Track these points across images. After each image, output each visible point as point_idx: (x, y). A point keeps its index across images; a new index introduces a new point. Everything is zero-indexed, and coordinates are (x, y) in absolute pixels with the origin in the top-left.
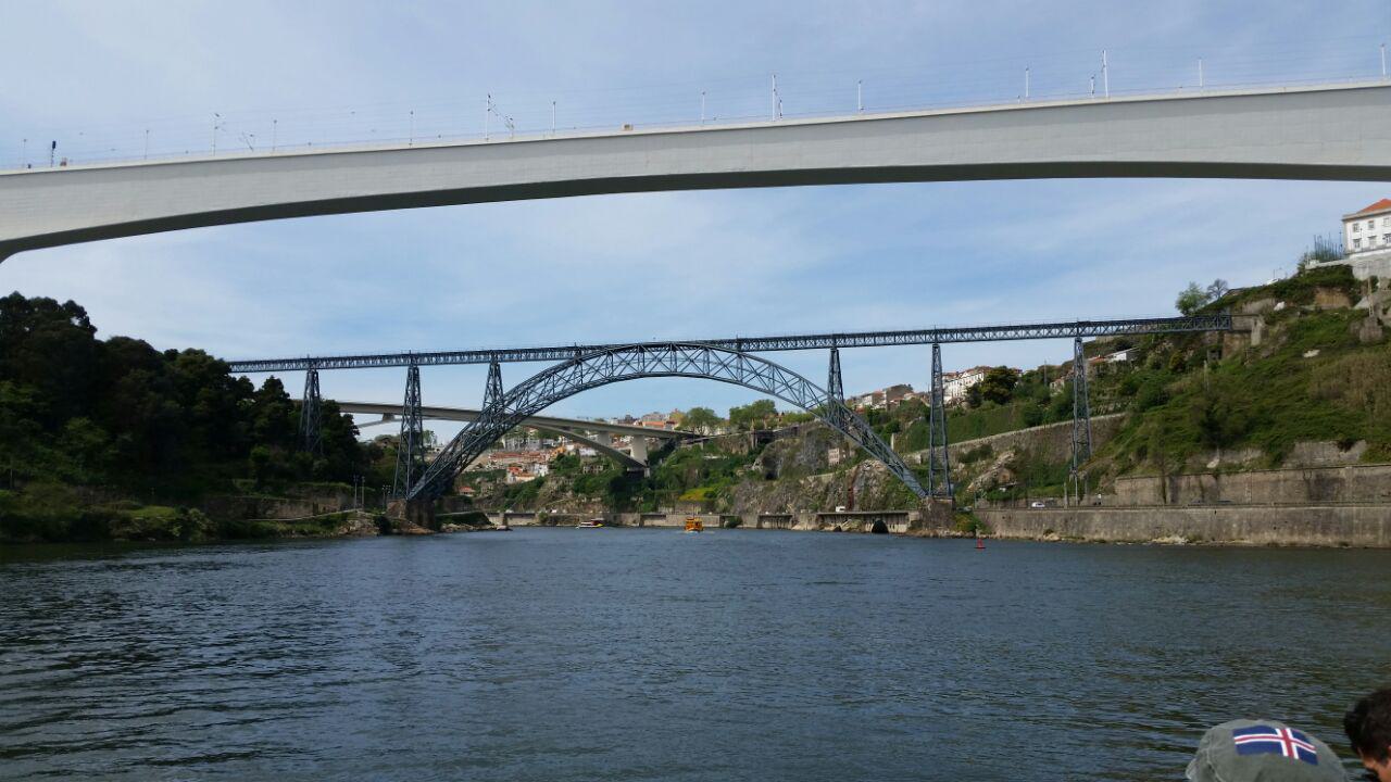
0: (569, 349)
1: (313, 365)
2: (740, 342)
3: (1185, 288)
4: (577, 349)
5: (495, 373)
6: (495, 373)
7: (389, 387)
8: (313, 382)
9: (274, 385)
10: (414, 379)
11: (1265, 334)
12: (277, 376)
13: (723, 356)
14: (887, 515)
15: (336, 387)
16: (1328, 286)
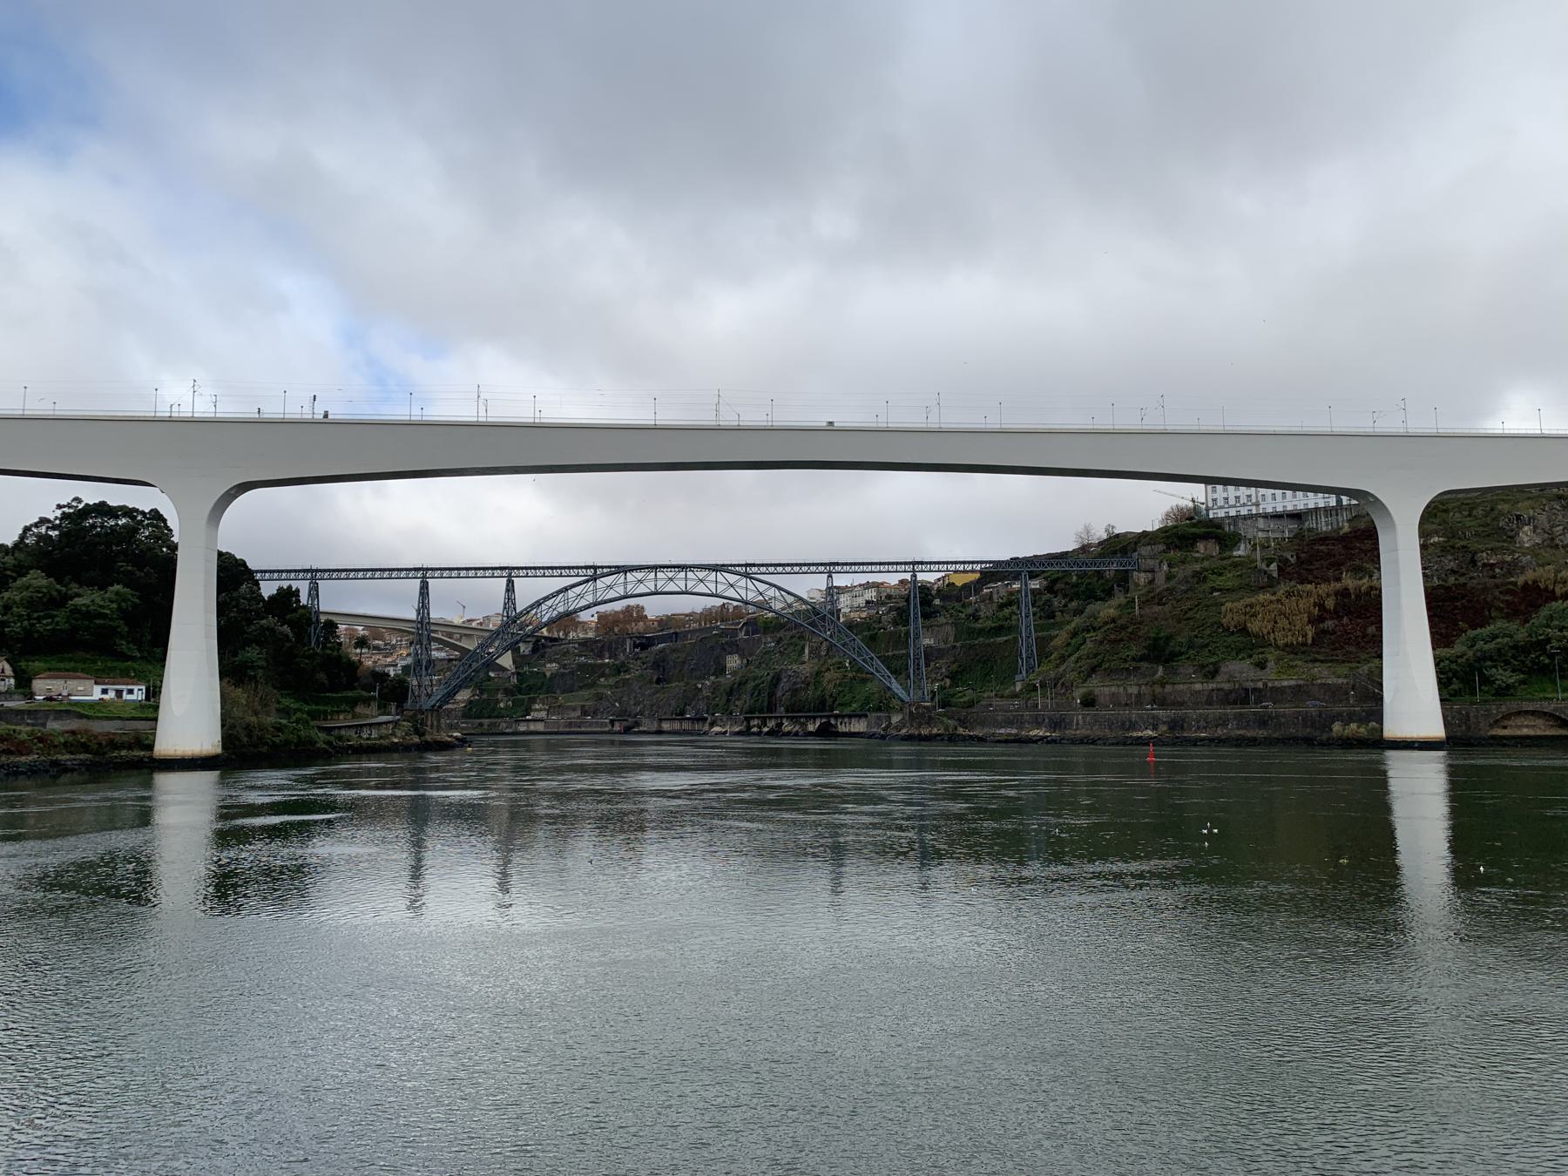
0: (587, 567)
1: (314, 575)
2: (747, 565)
3: (1080, 529)
4: (595, 568)
5: (510, 588)
6: (510, 588)
7: (398, 603)
8: (314, 592)
9: (288, 595)
10: (424, 590)
11: (1169, 578)
12: (295, 585)
13: (732, 578)
14: (836, 717)
15: (334, 600)
16: (1205, 537)
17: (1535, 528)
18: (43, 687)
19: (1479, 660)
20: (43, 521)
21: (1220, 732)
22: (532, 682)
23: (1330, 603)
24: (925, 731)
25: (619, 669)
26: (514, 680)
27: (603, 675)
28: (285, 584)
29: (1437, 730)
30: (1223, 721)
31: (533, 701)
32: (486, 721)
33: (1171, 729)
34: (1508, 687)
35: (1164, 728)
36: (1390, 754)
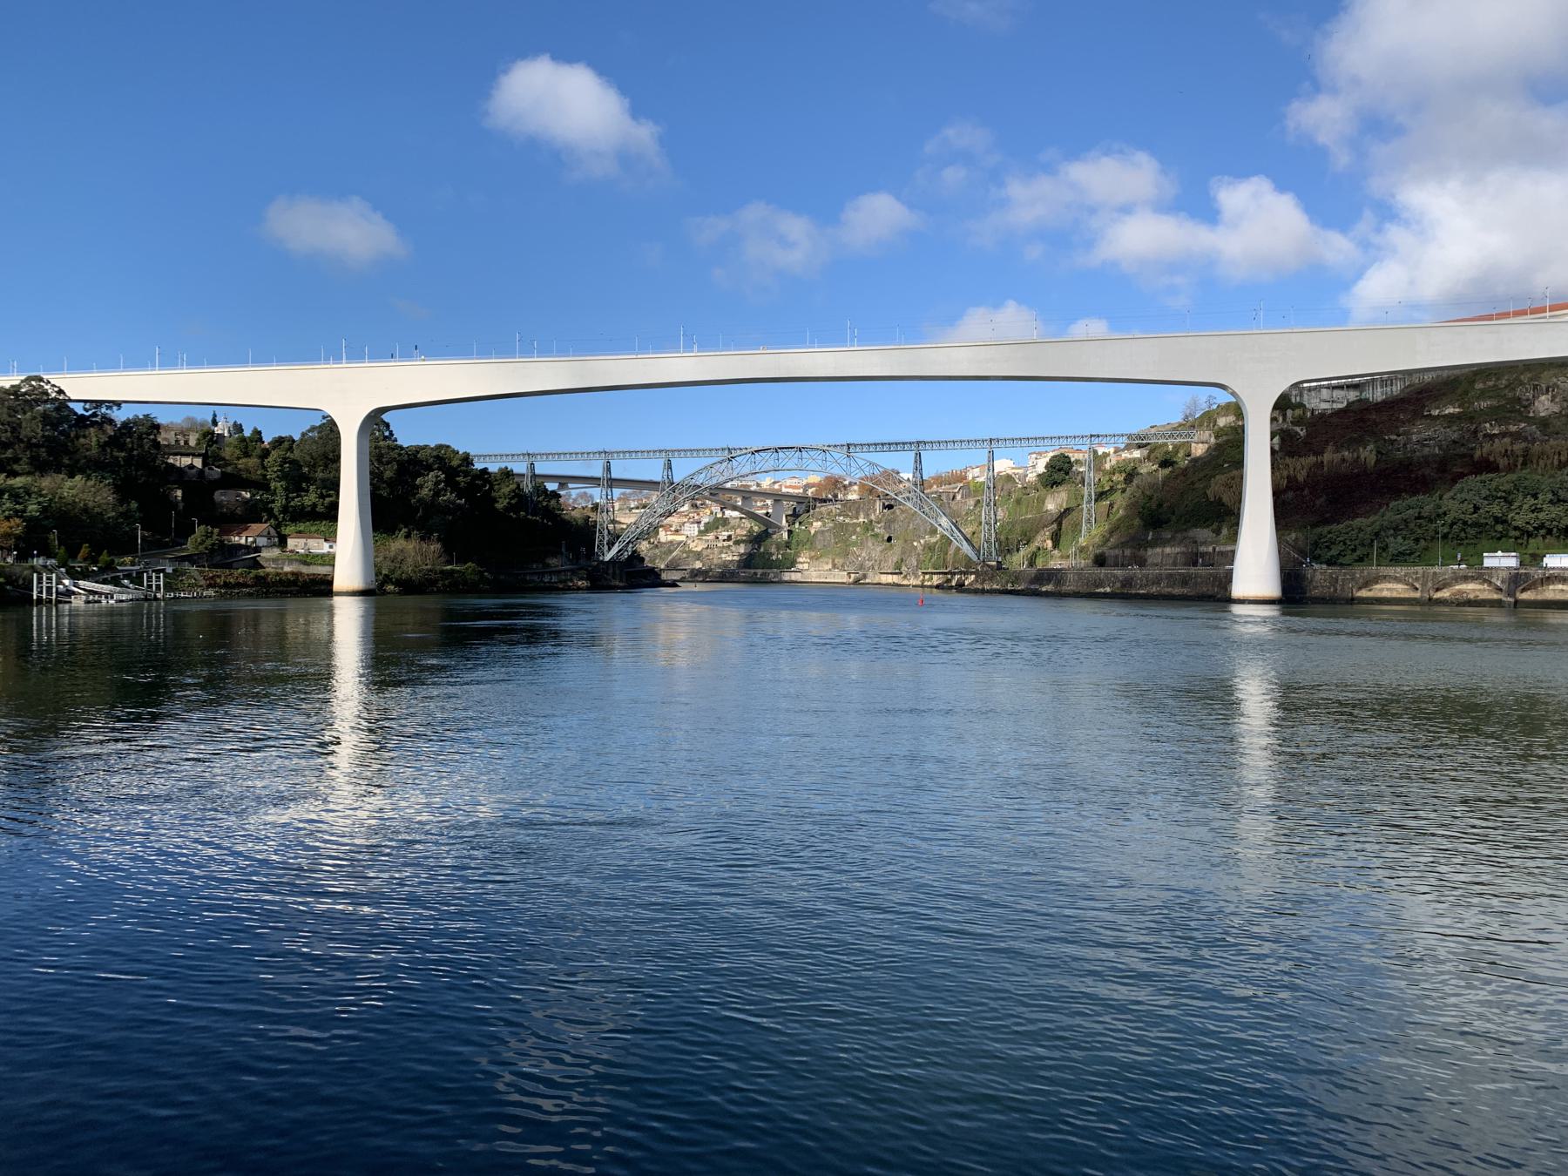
2: (848, 446)
17: (1554, 397)
18: (291, 543)
19: (1382, 528)
20: (313, 429)
21: (1154, 589)
22: (802, 536)
23: (1301, 478)
24: (987, 587)
25: (868, 526)
26: (785, 536)
27: (855, 532)
28: (503, 466)
29: (1272, 589)
30: (1157, 581)
31: (797, 554)
32: (760, 571)
33: (1123, 586)
34: (1401, 554)
35: (1118, 585)
36: (1237, 609)
